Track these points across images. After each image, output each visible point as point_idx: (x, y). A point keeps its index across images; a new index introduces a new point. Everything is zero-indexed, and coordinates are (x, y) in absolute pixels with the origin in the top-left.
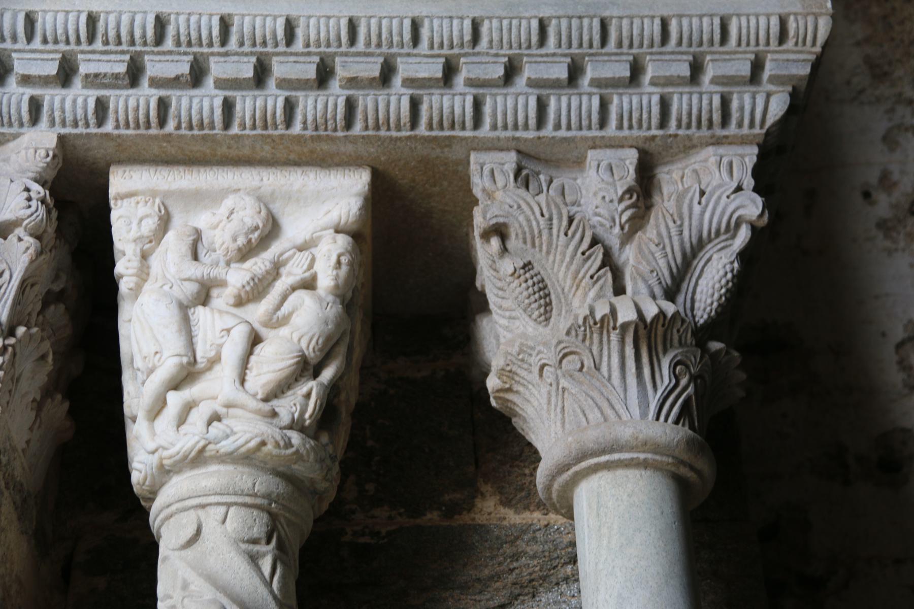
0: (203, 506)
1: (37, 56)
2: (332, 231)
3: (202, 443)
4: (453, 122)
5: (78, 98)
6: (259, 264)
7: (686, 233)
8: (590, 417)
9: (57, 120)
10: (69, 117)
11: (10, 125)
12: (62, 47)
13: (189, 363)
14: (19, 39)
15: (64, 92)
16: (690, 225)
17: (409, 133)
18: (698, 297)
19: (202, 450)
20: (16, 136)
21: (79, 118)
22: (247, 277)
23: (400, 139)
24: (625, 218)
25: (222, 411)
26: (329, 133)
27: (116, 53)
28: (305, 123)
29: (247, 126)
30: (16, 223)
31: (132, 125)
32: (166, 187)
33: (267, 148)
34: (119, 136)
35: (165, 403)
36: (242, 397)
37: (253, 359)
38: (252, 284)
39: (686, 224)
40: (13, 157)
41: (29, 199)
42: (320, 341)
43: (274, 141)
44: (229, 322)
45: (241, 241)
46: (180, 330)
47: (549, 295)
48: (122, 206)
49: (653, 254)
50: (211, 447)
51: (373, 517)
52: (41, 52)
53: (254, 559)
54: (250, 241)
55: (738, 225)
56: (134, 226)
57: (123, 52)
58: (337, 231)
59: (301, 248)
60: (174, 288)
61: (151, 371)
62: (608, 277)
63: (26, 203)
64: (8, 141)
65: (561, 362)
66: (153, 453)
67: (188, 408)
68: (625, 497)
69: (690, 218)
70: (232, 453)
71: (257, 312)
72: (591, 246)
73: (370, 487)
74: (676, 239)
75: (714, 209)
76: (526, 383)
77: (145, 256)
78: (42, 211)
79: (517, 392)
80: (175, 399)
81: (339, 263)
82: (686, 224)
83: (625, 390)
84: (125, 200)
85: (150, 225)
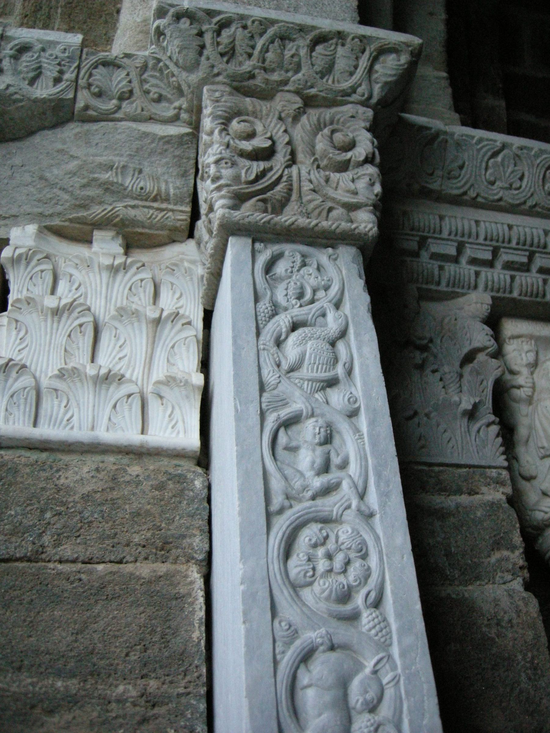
1: (480, 247)
5: (498, 275)
9: (490, 287)
10: (496, 286)
11: (463, 287)
12: (494, 243)
14: (472, 237)
15: (492, 270)
20: (463, 295)
21: (501, 287)
27: (522, 250)
31: (529, 294)
32: (538, 334)
34: (520, 301)
40: (466, 308)
52: (482, 245)
57: (526, 250)
64: (458, 297)
84: (515, 340)
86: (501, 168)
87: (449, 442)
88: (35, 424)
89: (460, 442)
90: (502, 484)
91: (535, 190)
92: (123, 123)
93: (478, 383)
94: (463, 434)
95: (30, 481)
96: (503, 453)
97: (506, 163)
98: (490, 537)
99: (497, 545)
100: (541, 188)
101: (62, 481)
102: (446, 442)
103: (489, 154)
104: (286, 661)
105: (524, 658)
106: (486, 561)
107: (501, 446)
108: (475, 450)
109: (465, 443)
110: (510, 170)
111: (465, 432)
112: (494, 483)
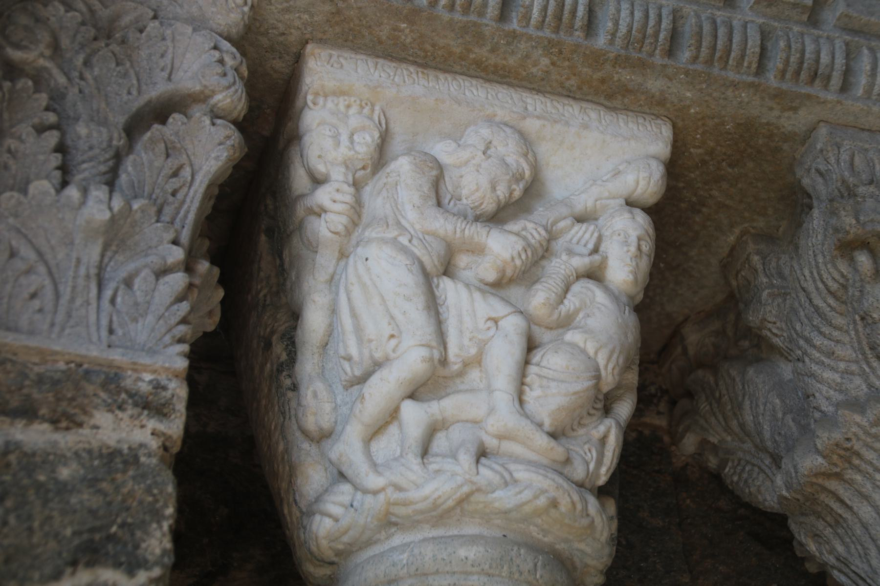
2: (623, 202)
3: (466, 489)
4: (816, 74)
17: (751, 79)
22: (519, 245)
23: (735, 85)
25: (491, 443)
26: (643, 55)
29: (533, 22)
30: (200, 98)
33: (545, 61)
36: (526, 428)
37: (532, 369)
38: (524, 257)
42: (621, 361)
43: (561, 52)
44: (499, 308)
48: (324, 106)
50: (478, 497)
59: (580, 219)
60: (415, 241)
61: (377, 365)
66: (375, 493)
70: (506, 512)
71: (539, 299)
76: (870, 470)
78: (239, 86)
79: (850, 483)
80: (414, 415)
81: (639, 248)
85: (366, 143)
87: (33, 296)
89: (64, 300)
90: (160, 410)
93: (167, 171)
94: (81, 282)
96: (180, 341)
98: (75, 533)
102: (26, 295)
107: (184, 321)
108: (104, 322)
109: (79, 302)
111: (88, 276)
112: (136, 405)
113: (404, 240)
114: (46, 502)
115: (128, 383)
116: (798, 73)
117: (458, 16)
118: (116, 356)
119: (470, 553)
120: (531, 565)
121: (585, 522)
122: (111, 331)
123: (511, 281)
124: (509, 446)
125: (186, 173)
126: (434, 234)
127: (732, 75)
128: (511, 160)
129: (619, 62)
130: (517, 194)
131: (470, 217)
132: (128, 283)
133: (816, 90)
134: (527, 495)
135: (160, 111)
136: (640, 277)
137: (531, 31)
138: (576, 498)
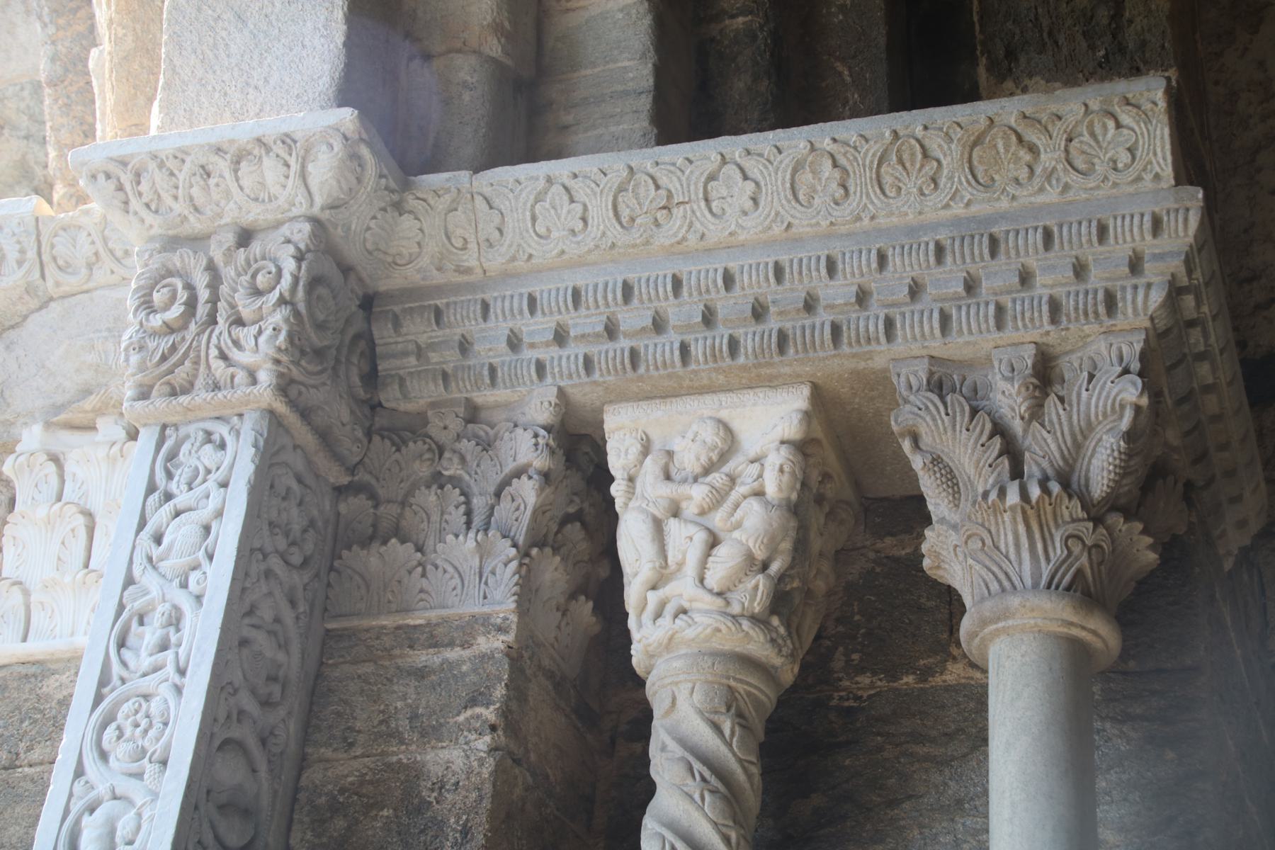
0: (677, 683)
6: (717, 478)
7: (1075, 417)
8: (992, 588)
13: (661, 567)
16: (1079, 410)
18: (1091, 475)
19: (671, 639)
20: (529, 392)
23: (824, 359)
24: (1023, 409)
25: (686, 605)
28: (746, 354)
33: (721, 377)
35: (646, 599)
39: (1075, 409)
41: (536, 445)
45: (704, 460)
46: (653, 540)
47: (957, 484)
49: (1045, 440)
51: (857, 683)
53: (717, 728)
54: (710, 459)
55: (1122, 407)
56: (623, 455)
58: (782, 442)
61: (636, 575)
62: (1005, 463)
63: (533, 449)
65: (966, 543)
67: (662, 606)
68: (1019, 658)
69: (1078, 404)
72: (991, 437)
73: (855, 656)
74: (1065, 424)
75: (1100, 394)
77: (631, 479)
80: (653, 598)
81: (781, 470)
82: (1075, 409)
83: (1020, 564)
86: (552, 212)
87: (454, 589)
88: (25, 639)
91: (606, 226)
92: (98, 292)
95: (15, 695)
97: (557, 202)
99: (473, 702)
100: (614, 221)
101: (45, 689)
103: (532, 197)
104: (75, 808)
105: (457, 822)
106: (451, 721)
107: (516, 584)
110: (564, 211)
113: (644, 506)
114: (457, 682)
115: (492, 620)
116: (858, 342)
117: (662, 372)
118: (486, 609)
119: (677, 664)
120: (710, 664)
121: (741, 635)
122: (485, 597)
123: (710, 509)
124: (696, 605)
125: (522, 507)
126: (662, 497)
127: (821, 354)
128: (709, 440)
129: (759, 365)
130: (715, 458)
131: (690, 480)
132: (493, 573)
133: (874, 347)
134: (700, 629)
135: (506, 482)
136: (784, 486)
137: (702, 366)
138: (730, 624)
